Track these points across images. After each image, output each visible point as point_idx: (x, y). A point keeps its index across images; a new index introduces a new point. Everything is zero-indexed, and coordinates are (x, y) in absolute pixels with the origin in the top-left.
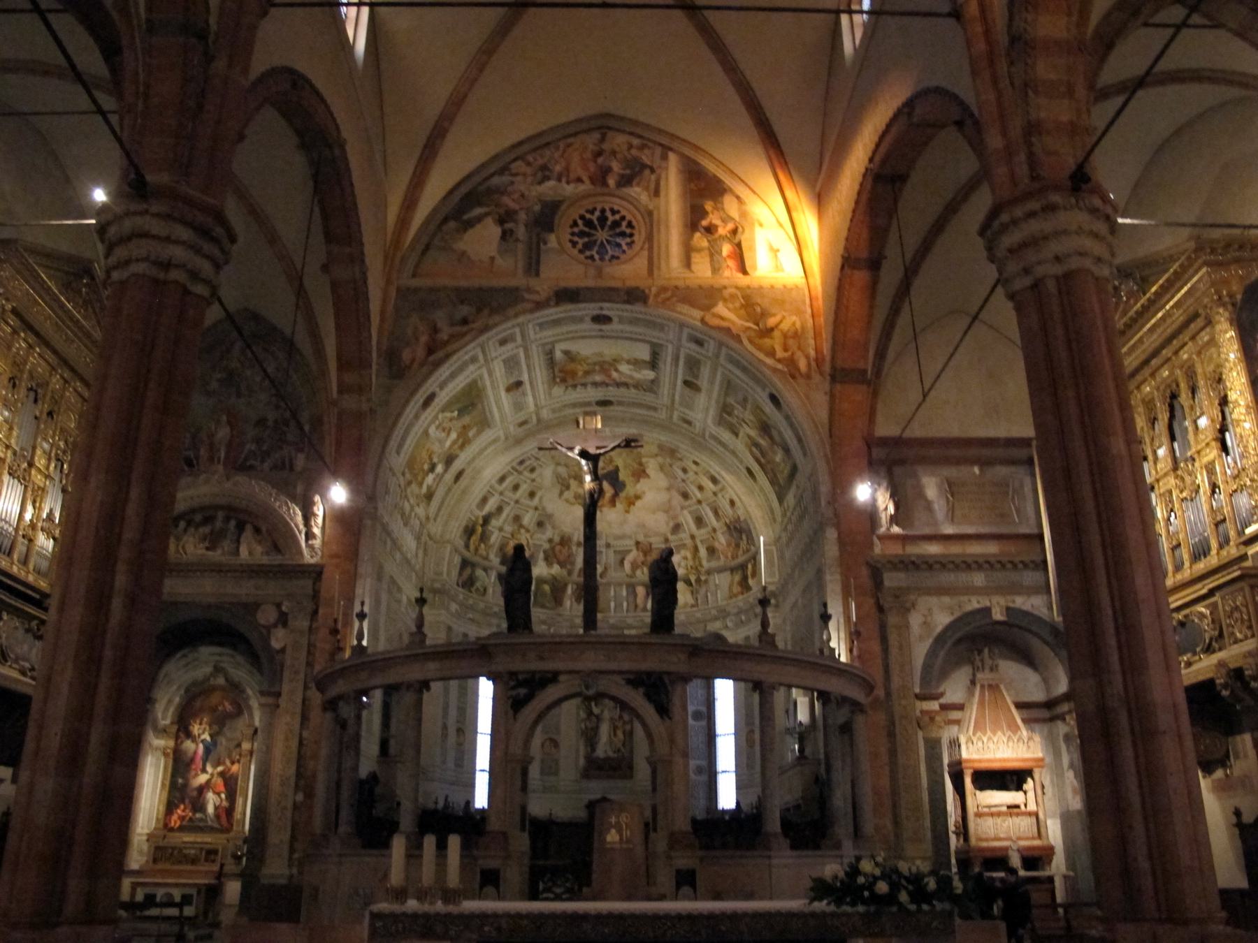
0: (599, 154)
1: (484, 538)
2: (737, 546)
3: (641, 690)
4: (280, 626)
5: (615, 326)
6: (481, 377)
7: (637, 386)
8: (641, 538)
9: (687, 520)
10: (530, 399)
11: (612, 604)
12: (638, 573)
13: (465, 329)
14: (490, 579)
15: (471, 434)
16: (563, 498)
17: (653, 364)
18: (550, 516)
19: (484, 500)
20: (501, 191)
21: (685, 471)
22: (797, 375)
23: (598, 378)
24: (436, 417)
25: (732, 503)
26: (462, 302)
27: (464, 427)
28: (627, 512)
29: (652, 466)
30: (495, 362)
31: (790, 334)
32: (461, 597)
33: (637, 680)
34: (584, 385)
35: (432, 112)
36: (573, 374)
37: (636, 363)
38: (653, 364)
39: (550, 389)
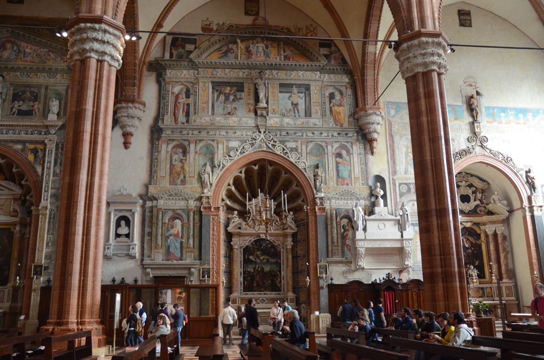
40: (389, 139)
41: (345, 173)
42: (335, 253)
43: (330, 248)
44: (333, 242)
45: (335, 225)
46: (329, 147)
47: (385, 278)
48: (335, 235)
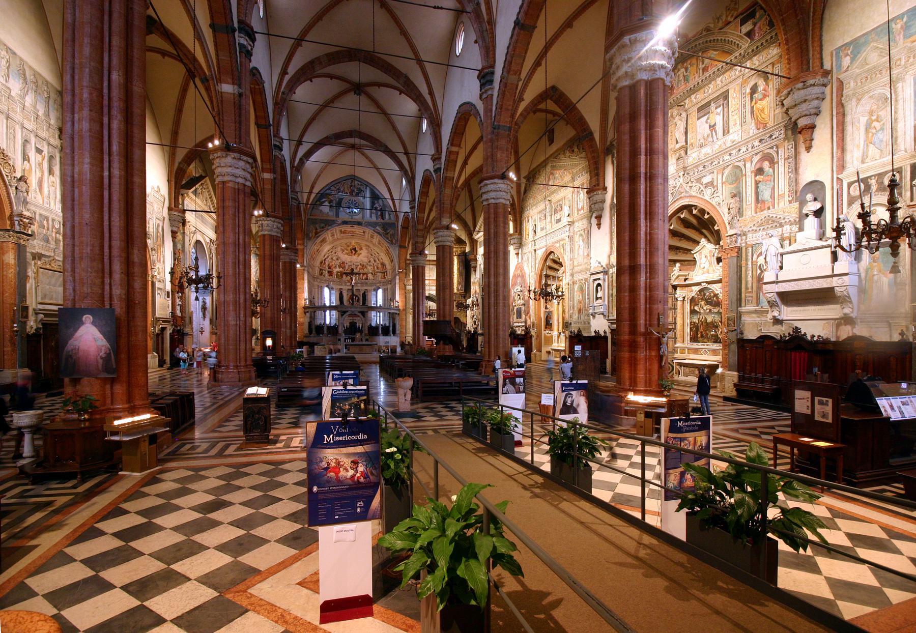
0: (351, 186)
17: (364, 232)
20: (329, 194)
29: (364, 248)
33: (360, 312)
35: (313, 179)
40: (837, 113)
41: (766, 195)
42: (748, 301)
43: (743, 295)
44: (747, 288)
45: (750, 266)
46: (748, 165)
47: (792, 333)
48: (750, 279)
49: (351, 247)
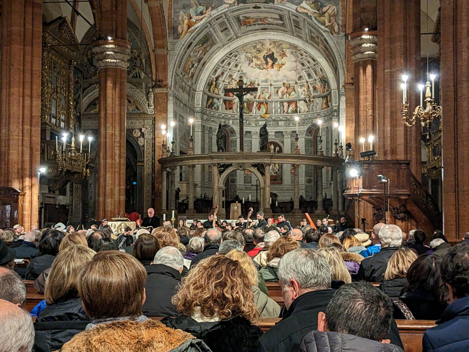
1: (216, 86)
2: (324, 87)
3: (256, 168)
4: (141, 137)
5: (263, 9)
6: (210, 31)
7: (277, 25)
8: (285, 82)
9: (304, 74)
10: (232, 32)
11: (274, 110)
12: (285, 96)
13: (203, 16)
14: (220, 103)
15: (208, 49)
16: (250, 65)
18: (245, 74)
19: (216, 71)
21: (302, 55)
22: (334, 33)
23: (259, 23)
24: (193, 49)
25: (321, 70)
26: (200, 5)
27: (205, 48)
28: (279, 71)
29: (288, 52)
30: (215, 25)
31: (332, 14)
32: (208, 112)
33: (255, 165)
34: (255, 25)
36: (249, 22)
37: (274, 18)
38: (281, 18)
39: (240, 27)
49: (264, 53)
